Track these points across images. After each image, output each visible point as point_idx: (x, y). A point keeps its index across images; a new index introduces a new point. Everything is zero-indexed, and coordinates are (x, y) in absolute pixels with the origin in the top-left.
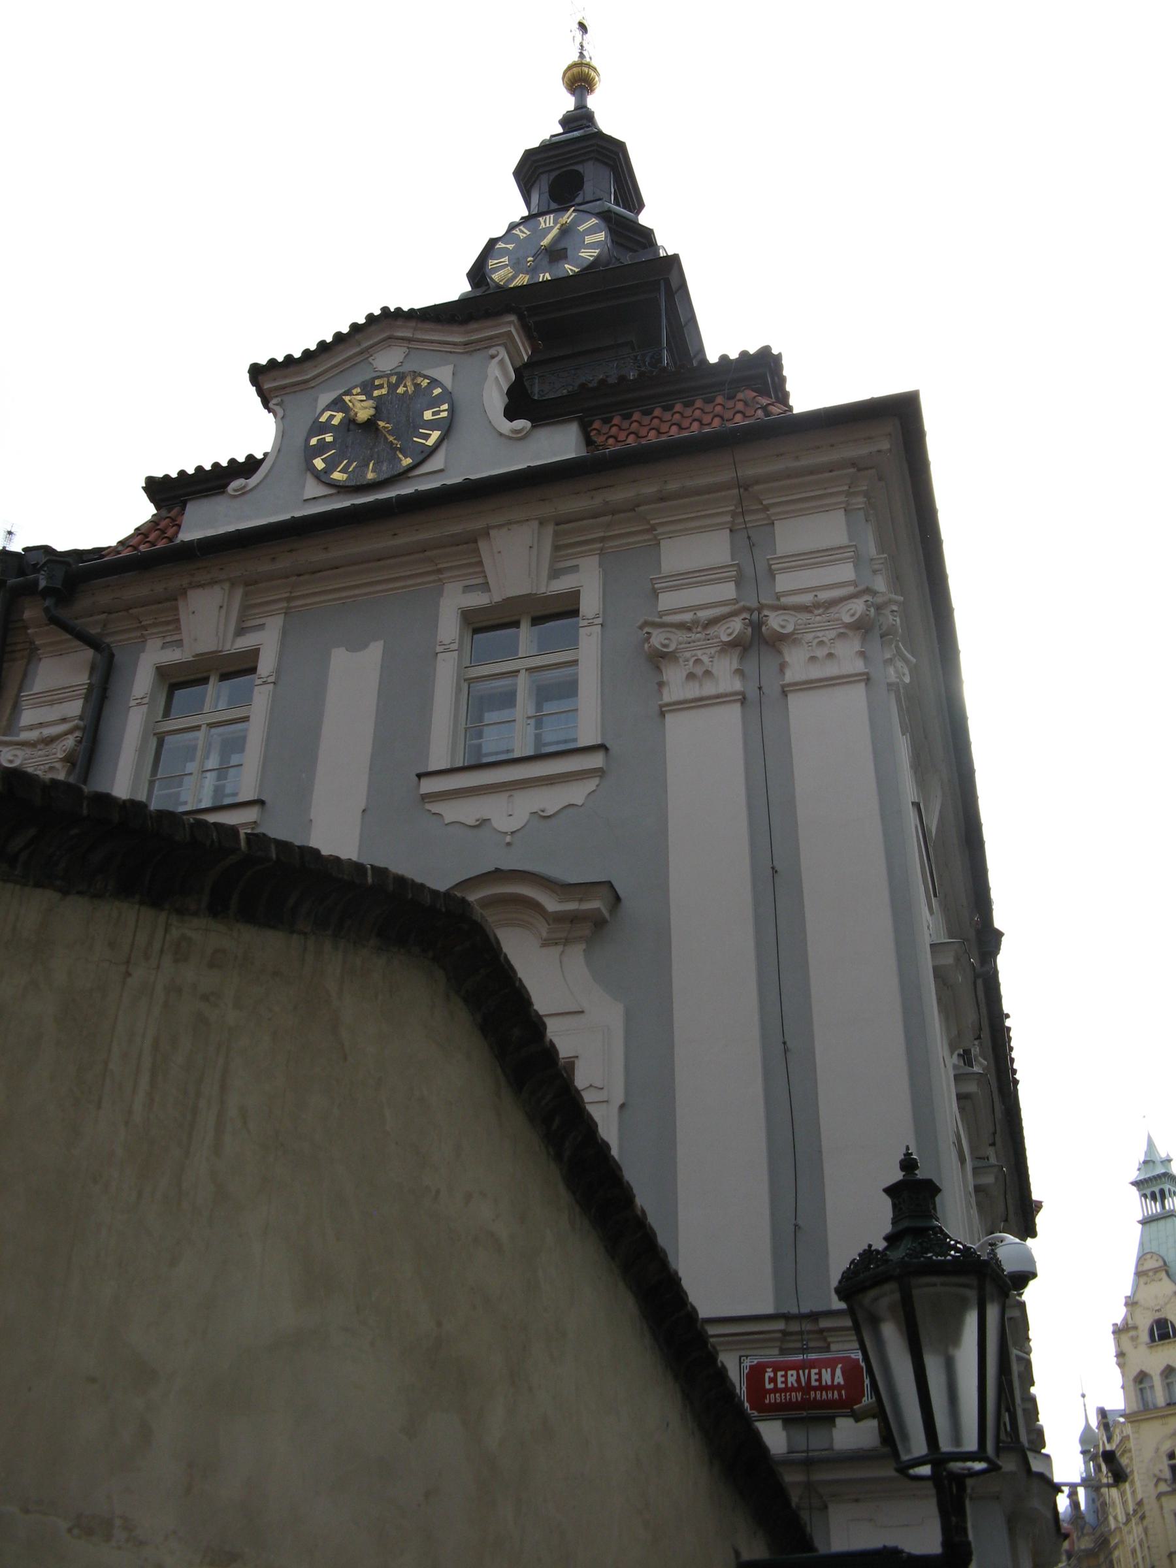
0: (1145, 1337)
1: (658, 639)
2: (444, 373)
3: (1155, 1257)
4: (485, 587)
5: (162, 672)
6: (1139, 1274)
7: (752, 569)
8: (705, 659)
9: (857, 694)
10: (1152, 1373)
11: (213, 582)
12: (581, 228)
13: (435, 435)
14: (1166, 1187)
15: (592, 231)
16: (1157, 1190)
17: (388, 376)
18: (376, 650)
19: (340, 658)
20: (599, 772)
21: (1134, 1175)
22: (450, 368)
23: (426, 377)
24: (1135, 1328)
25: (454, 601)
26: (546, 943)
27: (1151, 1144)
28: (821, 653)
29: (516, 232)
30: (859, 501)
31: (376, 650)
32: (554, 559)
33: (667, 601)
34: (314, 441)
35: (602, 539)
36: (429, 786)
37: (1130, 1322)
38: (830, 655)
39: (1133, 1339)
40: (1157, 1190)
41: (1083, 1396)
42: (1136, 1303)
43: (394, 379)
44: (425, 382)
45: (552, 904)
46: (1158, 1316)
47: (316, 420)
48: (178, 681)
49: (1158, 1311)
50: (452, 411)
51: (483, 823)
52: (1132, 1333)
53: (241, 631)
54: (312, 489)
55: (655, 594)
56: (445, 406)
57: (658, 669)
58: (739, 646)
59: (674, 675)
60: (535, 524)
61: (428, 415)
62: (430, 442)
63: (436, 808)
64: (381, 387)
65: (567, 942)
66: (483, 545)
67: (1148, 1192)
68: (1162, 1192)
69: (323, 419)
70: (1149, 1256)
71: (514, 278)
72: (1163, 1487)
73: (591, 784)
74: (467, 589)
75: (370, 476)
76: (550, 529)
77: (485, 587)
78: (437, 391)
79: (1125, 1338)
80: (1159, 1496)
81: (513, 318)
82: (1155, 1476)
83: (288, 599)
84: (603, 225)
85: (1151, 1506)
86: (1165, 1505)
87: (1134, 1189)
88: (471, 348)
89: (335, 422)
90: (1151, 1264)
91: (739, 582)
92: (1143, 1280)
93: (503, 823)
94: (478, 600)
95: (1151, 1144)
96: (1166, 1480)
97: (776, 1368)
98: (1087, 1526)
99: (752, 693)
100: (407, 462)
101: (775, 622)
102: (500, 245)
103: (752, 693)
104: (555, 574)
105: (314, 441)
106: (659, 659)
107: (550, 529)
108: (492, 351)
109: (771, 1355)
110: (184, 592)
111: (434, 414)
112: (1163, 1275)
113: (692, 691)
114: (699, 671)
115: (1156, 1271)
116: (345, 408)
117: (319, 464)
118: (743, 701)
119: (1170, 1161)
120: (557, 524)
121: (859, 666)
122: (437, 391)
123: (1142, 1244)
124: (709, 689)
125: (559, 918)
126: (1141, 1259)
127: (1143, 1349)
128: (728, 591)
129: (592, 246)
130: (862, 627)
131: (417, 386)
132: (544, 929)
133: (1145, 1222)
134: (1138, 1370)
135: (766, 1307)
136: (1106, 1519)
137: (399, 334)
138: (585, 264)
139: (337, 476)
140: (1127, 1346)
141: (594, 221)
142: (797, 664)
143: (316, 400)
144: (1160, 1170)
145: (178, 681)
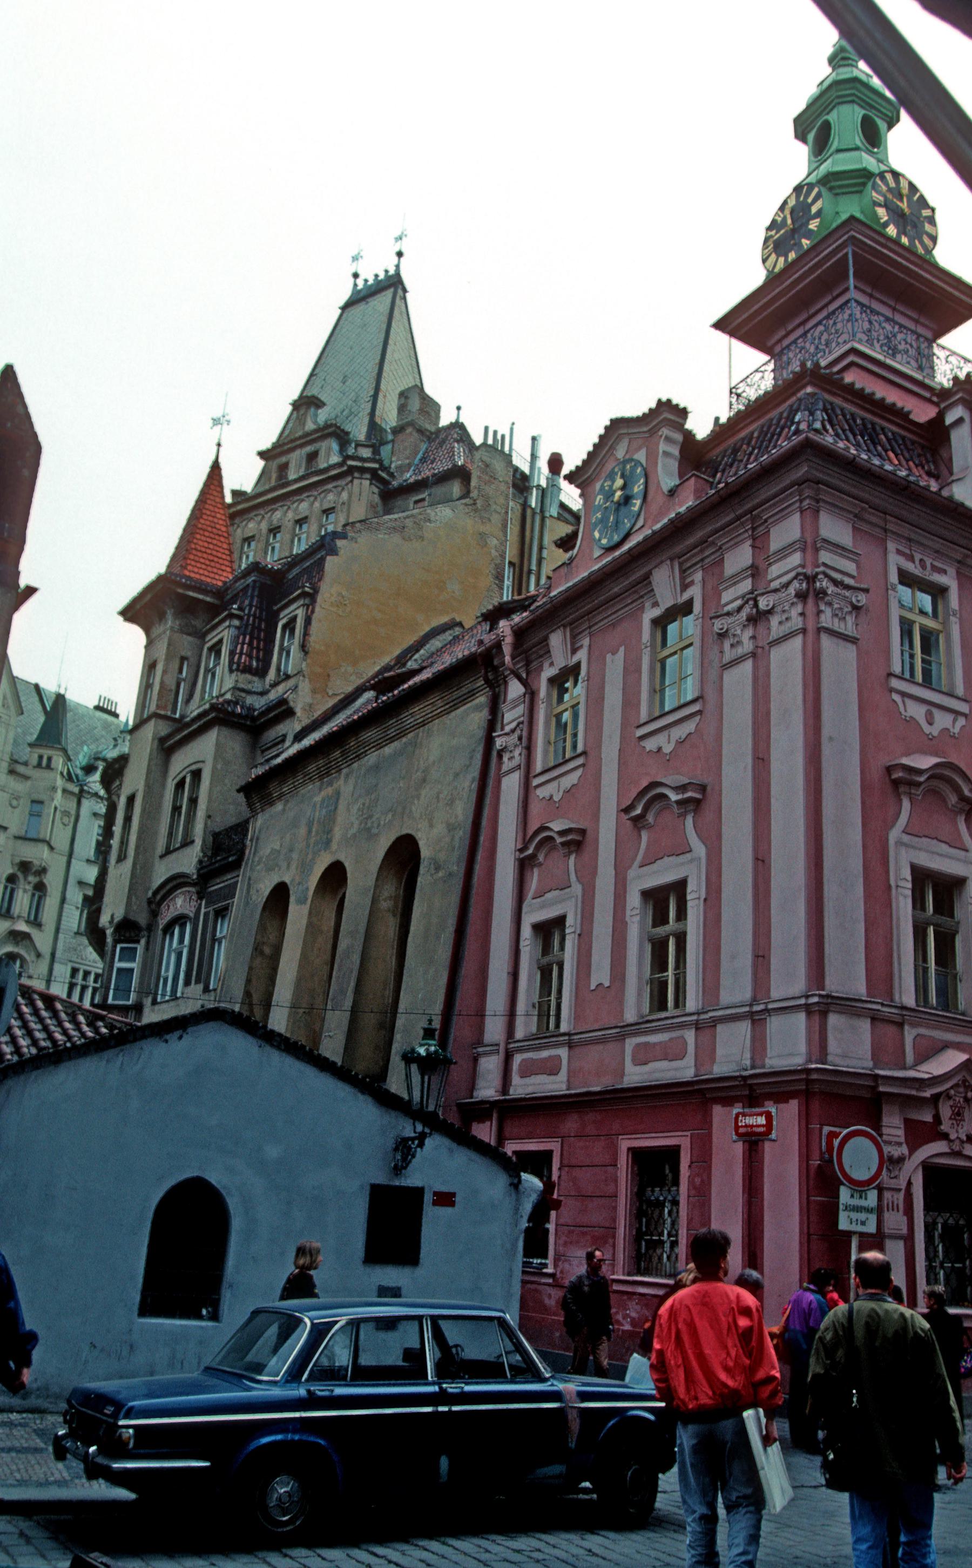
5: (551, 681)
8: (739, 632)
20: (700, 712)
35: (702, 560)
38: (787, 619)
48: (558, 683)
57: (722, 643)
60: (668, 562)
63: (643, 743)
73: (697, 718)
83: (590, 627)
91: (753, 576)
93: (667, 749)
94: (657, 612)
106: (722, 635)
108: (660, 433)
120: (679, 558)
130: (802, 596)
137: (622, 432)
142: (775, 626)
145: (558, 683)
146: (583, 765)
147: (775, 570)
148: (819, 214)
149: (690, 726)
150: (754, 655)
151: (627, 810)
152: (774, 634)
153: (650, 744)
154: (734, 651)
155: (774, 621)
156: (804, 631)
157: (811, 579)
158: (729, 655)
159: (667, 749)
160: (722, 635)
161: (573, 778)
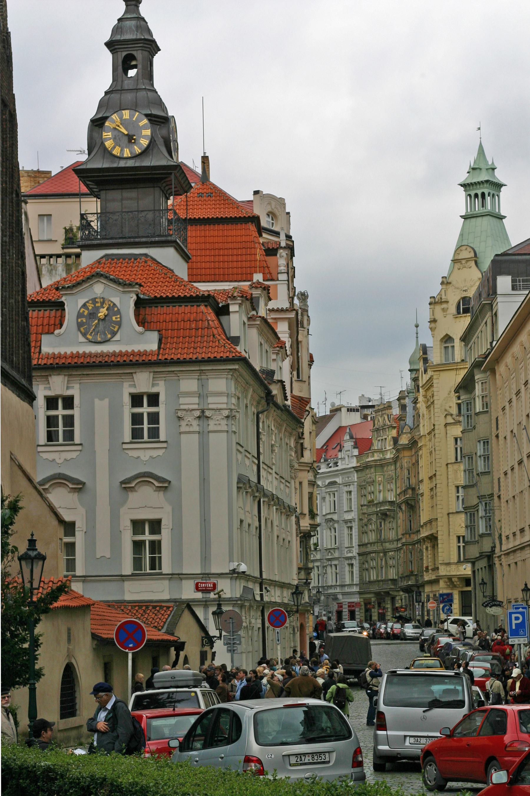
0: (453, 309)
1: (180, 414)
2: (116, 300)
3: (469, 249)
4: (134, 386)
6: (455, 261)
7: (202, 395)
9: (225, 434)
10: (454, 337)
11: (59, 375)
12: (141, 124)
13: (117, 327)
14: (486, 191)
15: (145, 127)
16: (479, 193)
17: (100, 298)
18: (107, 401)
19: (97, 401)
20: (166, 448)
21: (463, 177)
22: (118, 299)
23: (112, 302)
24: (447, 302)
25: (127, 390)
26: (155, 491)
27: (481, 150)
28: (217, 422)
29: (113, 117)
30: (230, 376)
31: (107, 401)
32: (153, 380)
33: (182, 400)
34: (79, 320)
36: (125, 446)
37: (443, 297)
39: (444, 310)
40: (479, 193)
41: (417, 326)
42: (450, 283)
43: (102, 300)
44: (112, 305)
45: (157, 484)
46: (464, 294)
47: (79, 312)
49: (465, 291)
50: (121, 318)
51: (138, 457)
52: (444, 306)
53: (68, 388)
54: (81, 339)
55: (179, 398)
56: (118, 316)
58: (199, 417)
59: (183, 423)
61: (114, 318)
62: (116, 330)
63: (127, 451)
64: (97, 302)
65: (159, 491)
66: (134, 375)
67: (473, 193)
68: (483, 194)
69: (81, 311)
70: (464, 248)
71: (114, 148)
72: (450, 420)
73: (164, 450)
74: (130, 386)
75: (99, 339)
76: (152, 374)
77: (134, 386)
78: (116, 309)
79: (438, 308)
80: (446, 425)
81: (137, 286)
82: (446, 410)
84: (149, 125)
85: (440, 429)
86: (448, 432)
87: (462, 189)
88: (124, 292)
89: (86, 313)
90: (466, 254)
91: (199, 397)
92: (457, 265)
95: (481, 150)
96: (452, 415)
97: (201, 583)
98: (406, 427)
99: (201, 431)
100: (109, 336)
101: (207, 413)
102: (107, 124)
103: (201, 431)
104: (153, 385)
105: (79, 320)
107: (152, 374)
109: (200, 581)
110: (51, 375)
111: (116, 318)
112: (473, 263)
113: (187, 429)
114: (189, 423)
115: (468, 260)
116: (88, 309)
117: (82, 329)
118: (199, 433)
119: (493, 169)
121: (225, 428)
122: (116, 309)
123: (461, 235)
124: (191, 429)
125: (158, 487)
126: (458, 249)
127: (450, 317)
128: (196, 400)
129: (145, 137)
130: (227, 417)
131: (109, 305)
132: (155, 488)
133: (465, 218)
134: (445, 334)
135: (199, 572)
136: (418, 425)
138: (143, 149)
139: (88, 336)
140: (439, 314)
141: (145, 121)
143: (77, 301)
144: (483, 177)
146: (81, 451)
147: (210, 400)
148: (145, 137)
149: (160, 452)
150: (199, 433)
151: (122, 483)
152: (212, 428)
153: (131, 453)
154: (188, 427)
155: (211, 422)
156: (227, 431)
157: (231, 410)
158: (184, 429)
159: (142, 458)
160: (179, 418)
161: (74, 455)
